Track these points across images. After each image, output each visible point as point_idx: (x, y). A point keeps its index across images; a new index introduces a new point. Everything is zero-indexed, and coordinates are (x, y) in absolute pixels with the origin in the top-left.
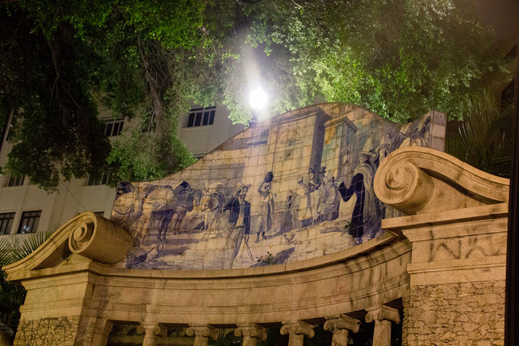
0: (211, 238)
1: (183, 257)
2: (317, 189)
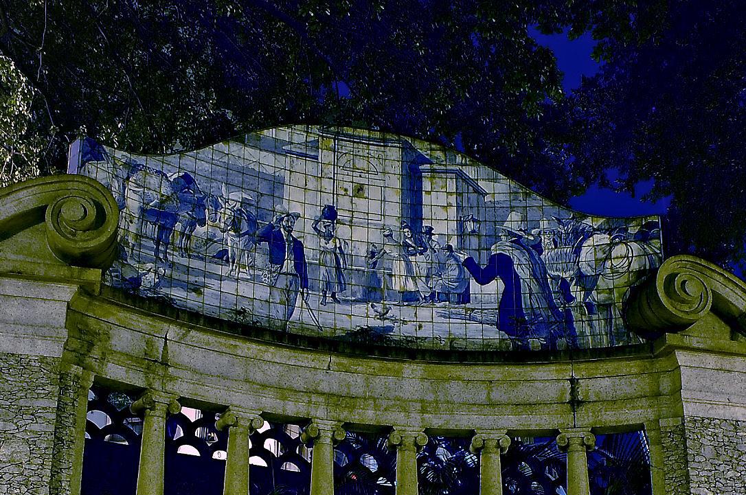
0: (243, 279)
1: (200, 299)
2: (421, 254)
